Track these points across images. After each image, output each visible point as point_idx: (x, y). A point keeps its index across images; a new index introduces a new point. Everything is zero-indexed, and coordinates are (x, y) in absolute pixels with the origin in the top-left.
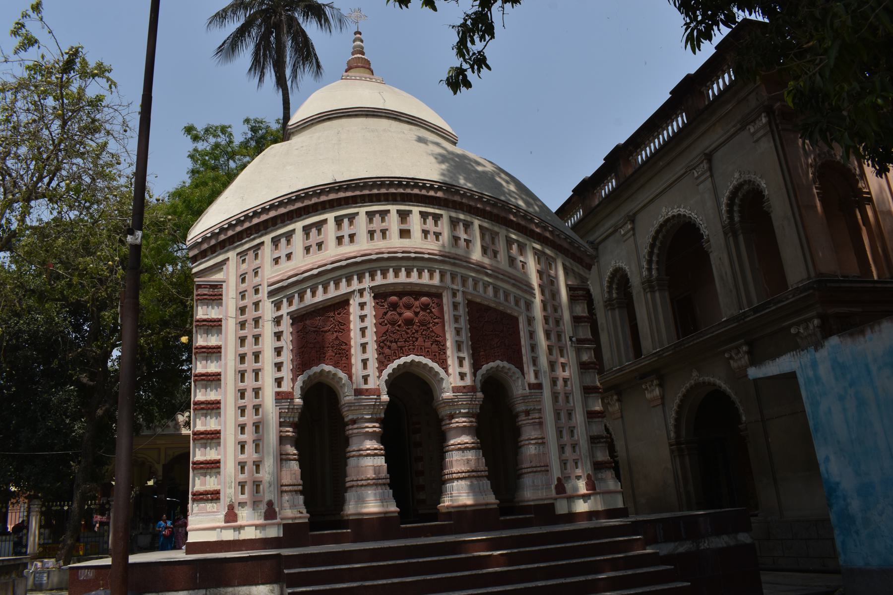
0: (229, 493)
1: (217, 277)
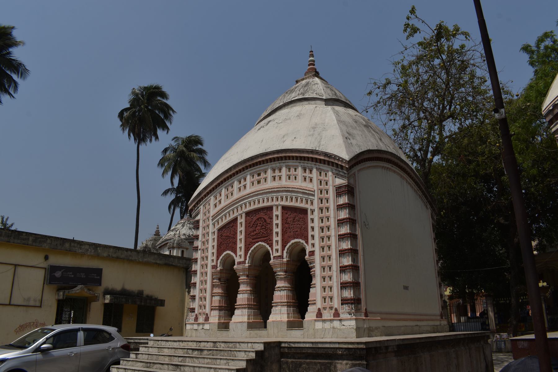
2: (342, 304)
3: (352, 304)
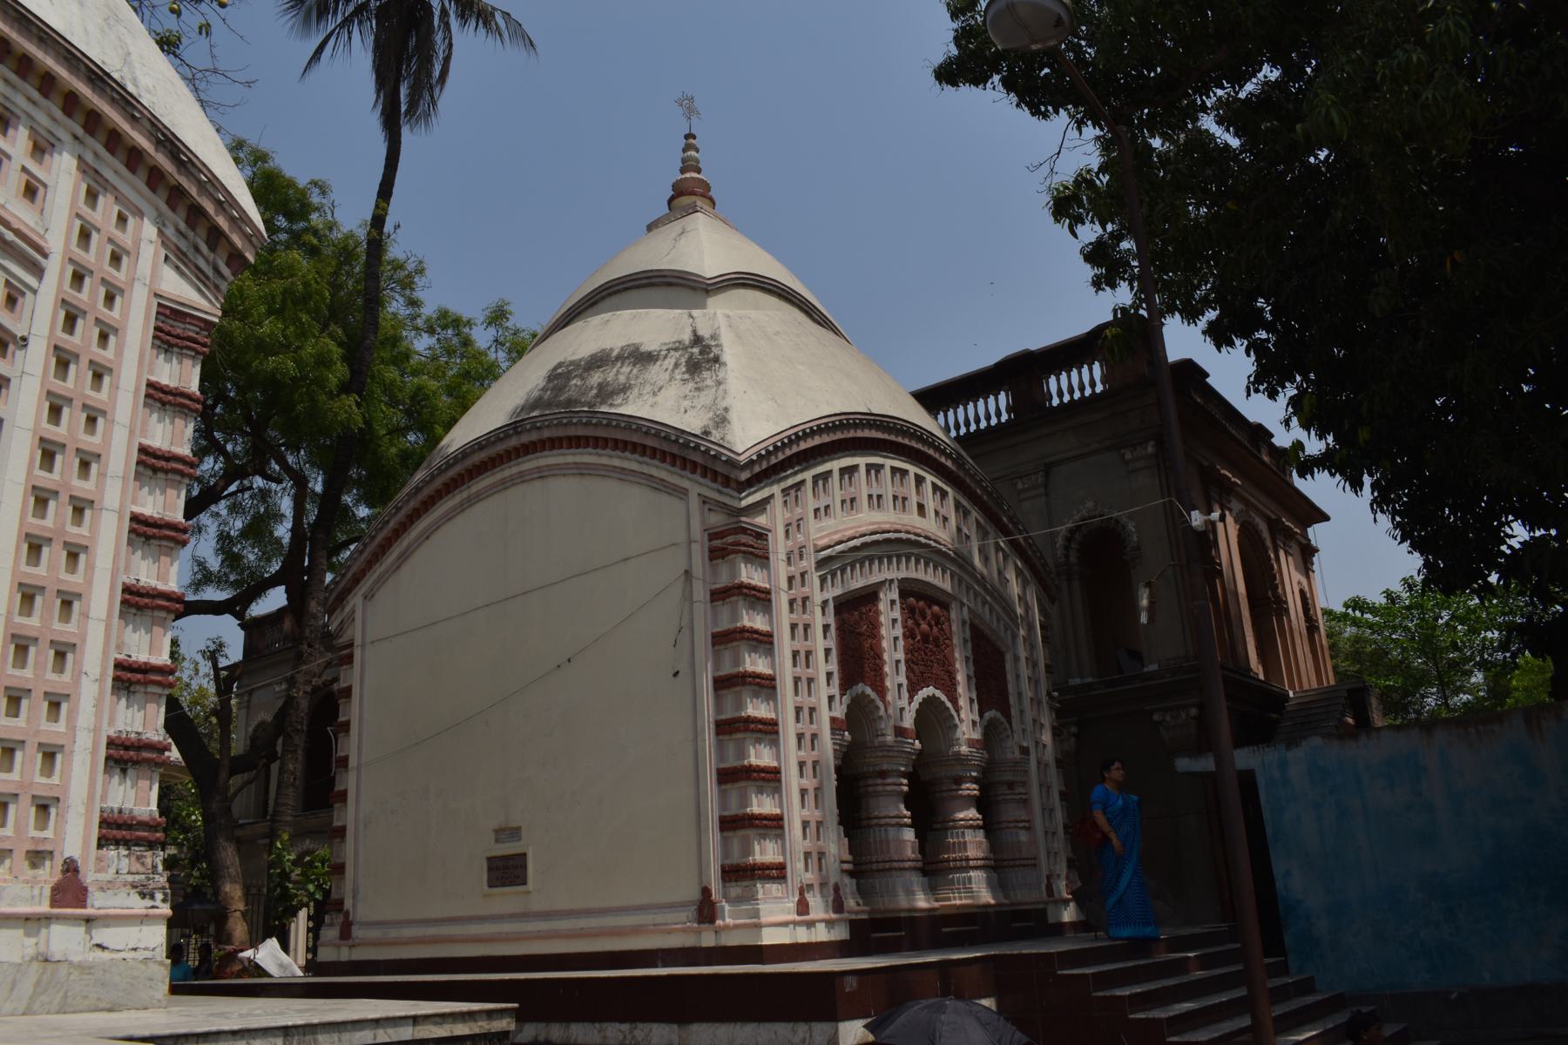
0: (799, 872)
1: (761, 520)
2: (102, 843)
3: (151, 845)
